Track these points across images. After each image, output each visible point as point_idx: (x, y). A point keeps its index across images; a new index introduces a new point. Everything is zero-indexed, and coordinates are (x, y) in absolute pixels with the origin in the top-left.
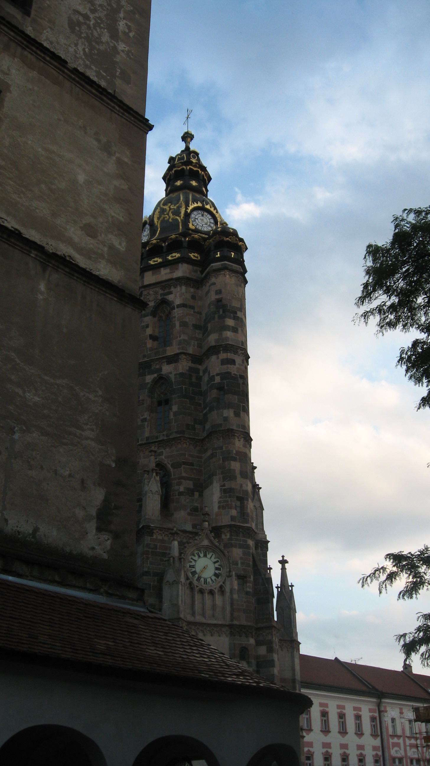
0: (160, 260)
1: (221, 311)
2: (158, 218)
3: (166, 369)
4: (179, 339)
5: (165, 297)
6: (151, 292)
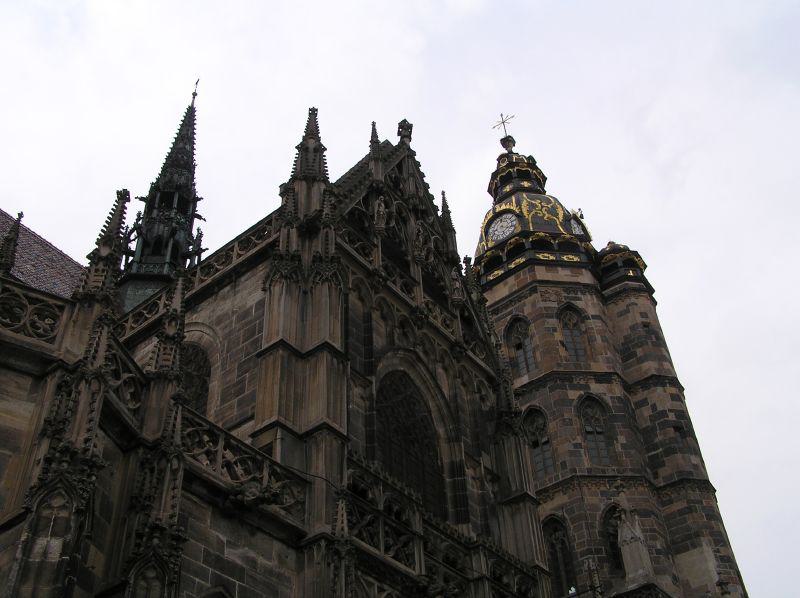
2: (529, 211)
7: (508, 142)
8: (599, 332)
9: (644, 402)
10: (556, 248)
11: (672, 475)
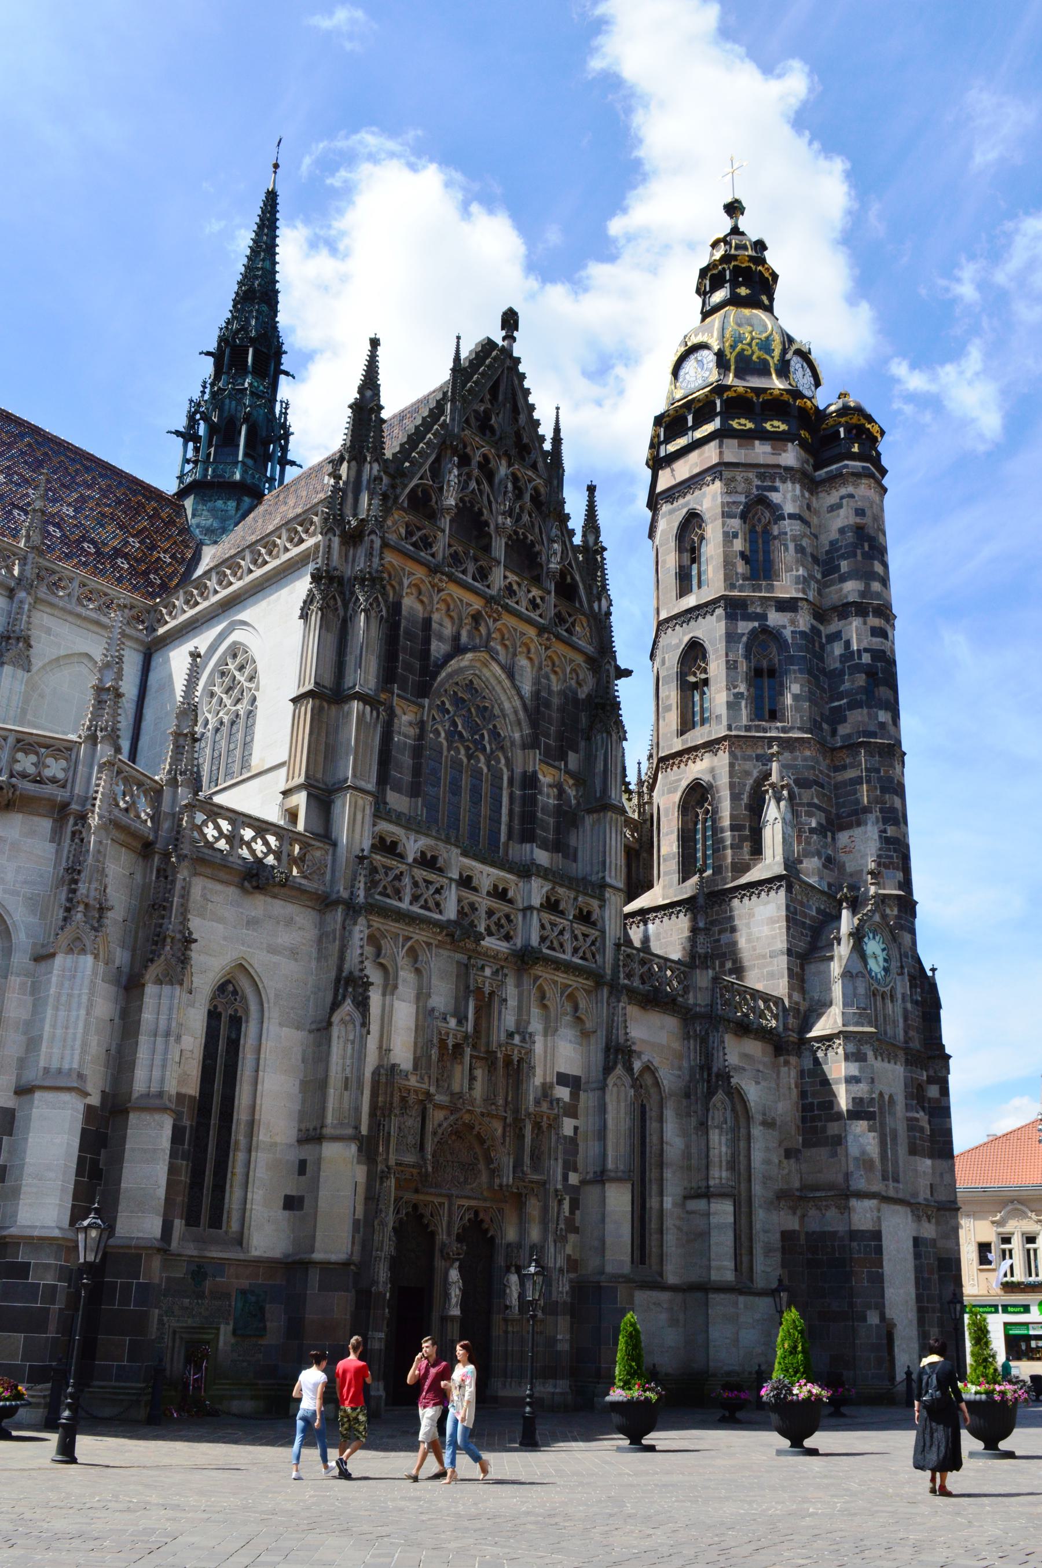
0: (750, 425)
1: (866, 547)
3: (775, 618)
4: (794, 573)
5: (766, 493)
6: (739, 478)
7: (733, 209)
8: (794, 539)
9: (836, 636)
10: (758, 410)
11: (849, 736)
